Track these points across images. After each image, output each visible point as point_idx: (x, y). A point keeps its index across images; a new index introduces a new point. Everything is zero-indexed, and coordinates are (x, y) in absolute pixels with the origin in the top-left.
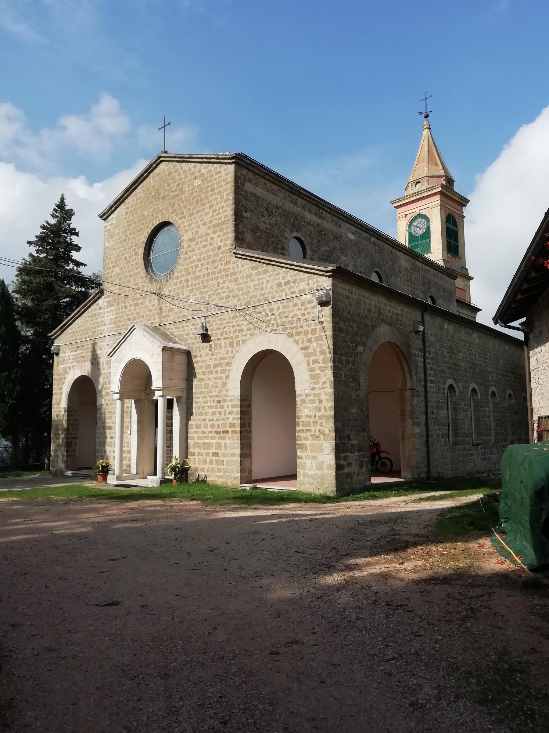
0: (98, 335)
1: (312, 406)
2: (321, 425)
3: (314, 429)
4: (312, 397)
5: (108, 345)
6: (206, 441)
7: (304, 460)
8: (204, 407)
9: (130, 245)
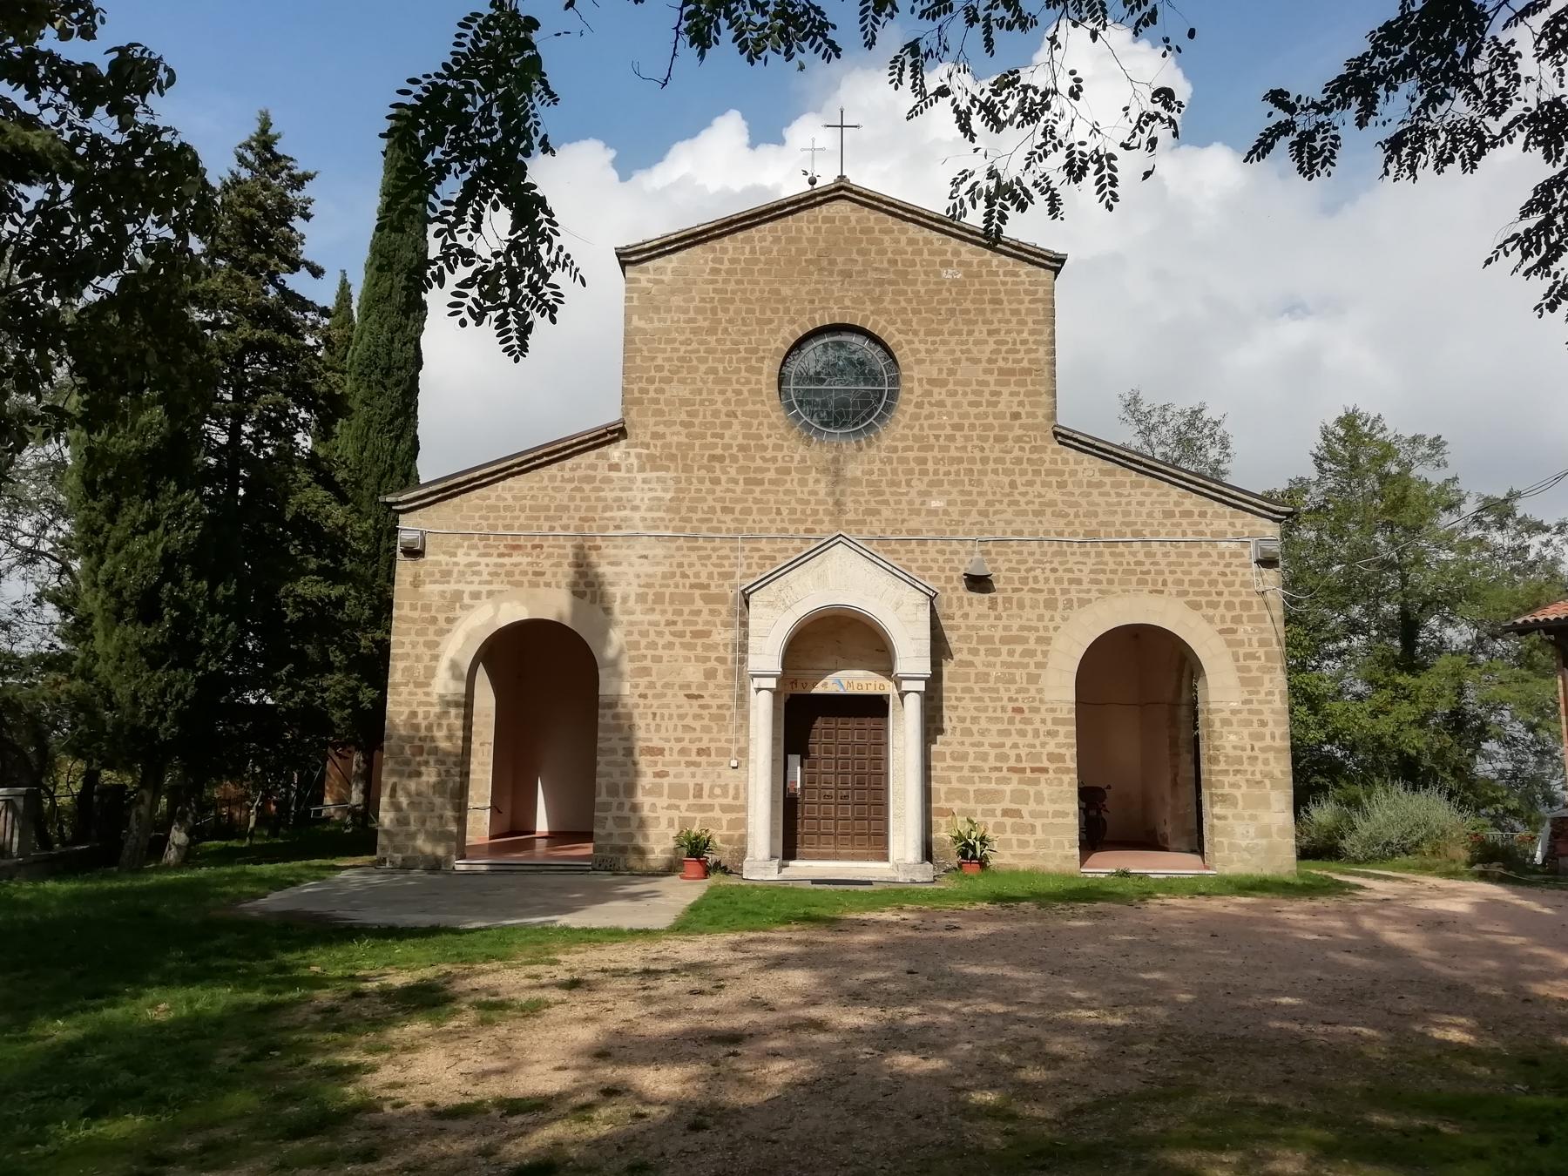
0: (606, 528)
1: (1246, 732)
2: (1266, 762)
3: (1250, 769)
4: (1245, 715)
5: (646, 557)
6: (984, 786)
7: (1231, 821)
8: (974, 720)
9: (728, 345)
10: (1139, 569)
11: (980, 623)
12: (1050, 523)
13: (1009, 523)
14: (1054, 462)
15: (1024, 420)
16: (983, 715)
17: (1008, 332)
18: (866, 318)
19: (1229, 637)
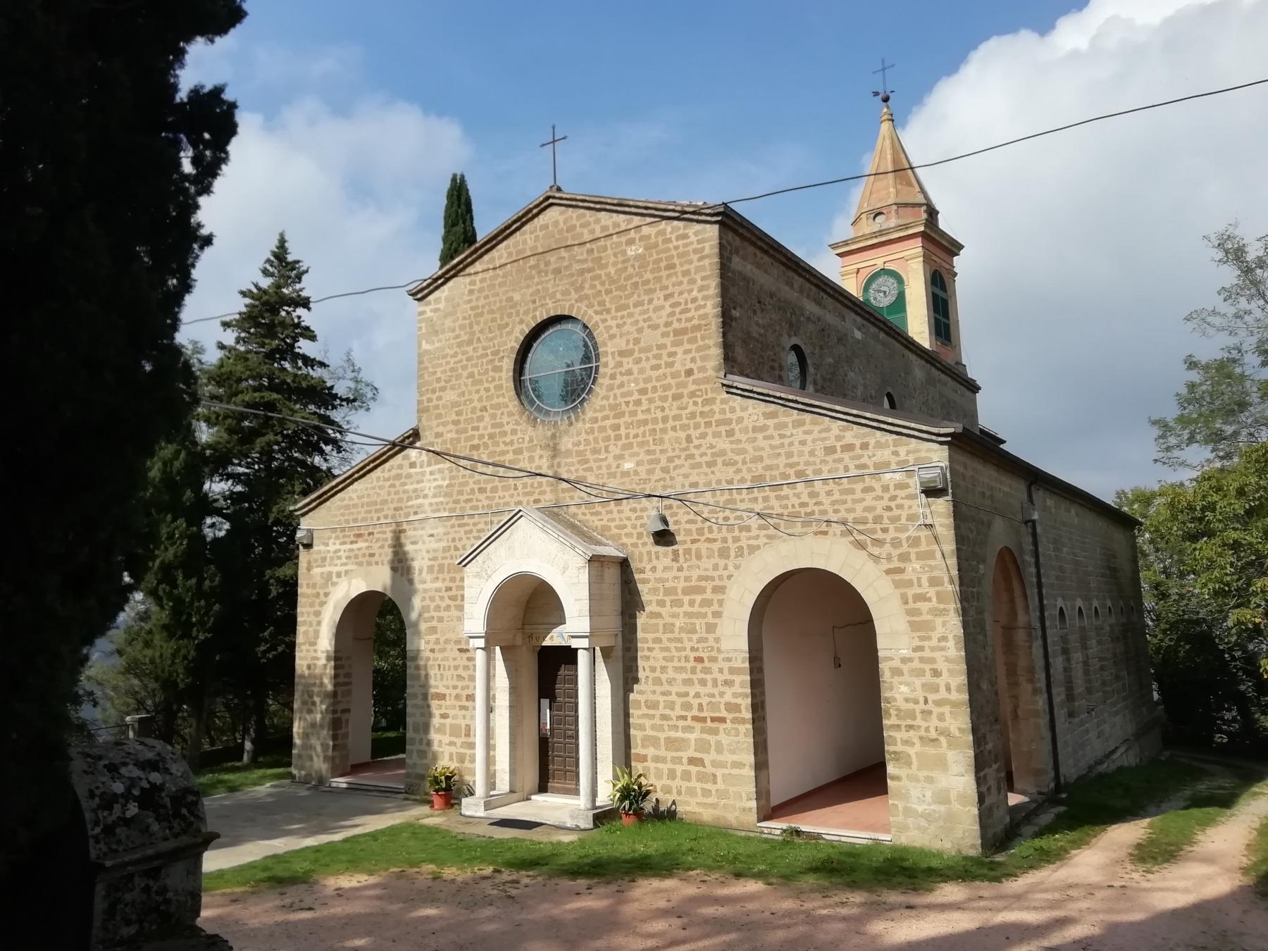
0: (407, 515)
1: (918, 682)
2: (941, 717)
3: (924, 724)
4: (916, 664)
5: (432, 535)
6: (673, 734)
7: (905, 782)
8: (663, 669)
9: (481, 352)
10: (803, 510)
11: (666, 575)
12: (722, 473)
13: (686, 476)
14: (723, 412)
15: (697, 375)
16: (670, 665)
17: (681, 293)
18: (572, 306)
19: (897, 577)
